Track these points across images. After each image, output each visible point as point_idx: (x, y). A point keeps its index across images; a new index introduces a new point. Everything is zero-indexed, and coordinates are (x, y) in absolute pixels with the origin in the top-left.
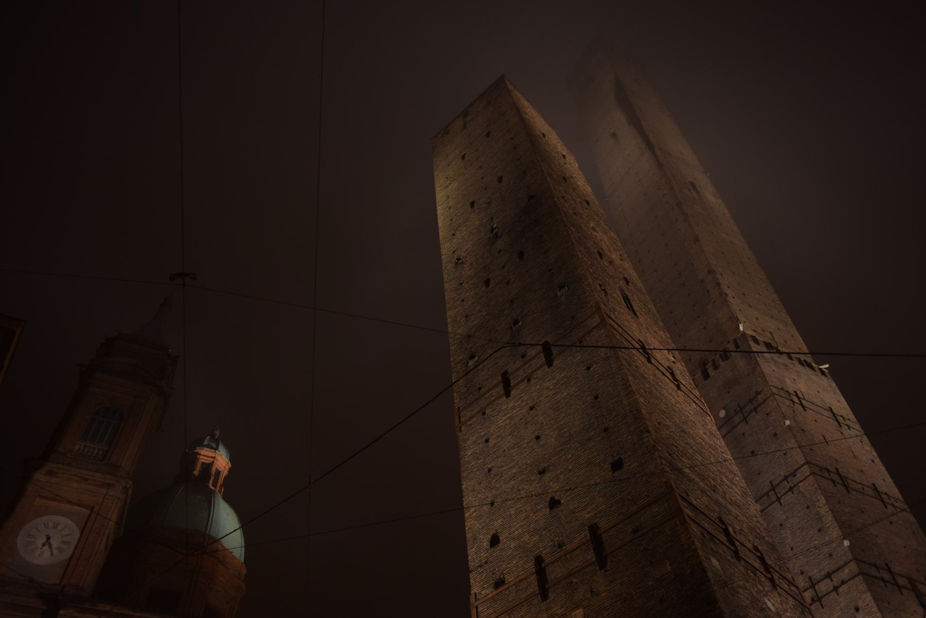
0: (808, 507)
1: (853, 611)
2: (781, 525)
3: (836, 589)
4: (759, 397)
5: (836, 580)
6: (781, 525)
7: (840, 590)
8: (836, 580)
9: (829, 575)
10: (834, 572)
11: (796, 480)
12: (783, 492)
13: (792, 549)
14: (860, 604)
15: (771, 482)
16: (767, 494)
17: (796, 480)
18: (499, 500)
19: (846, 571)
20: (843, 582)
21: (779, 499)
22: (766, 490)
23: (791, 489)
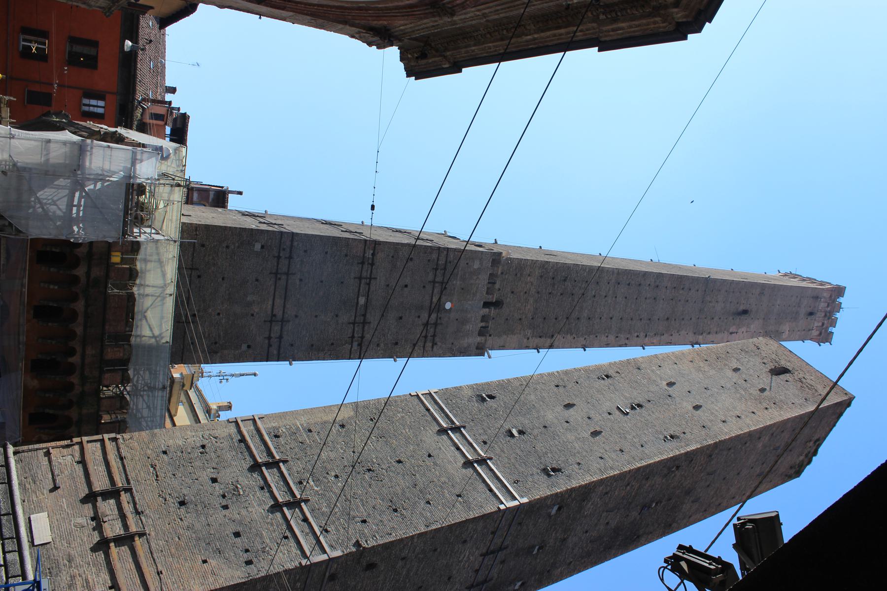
0: (332, 344)
1: (250, 343)
2: (337, 316)
3: (269, 338)
4: (431, 344)
5: (274, 341)
6: (337, 316)
7: (267, 341)
8: (274, 341)
9: (280, 337)
10: (280, 342)
11: (355, 344)
12: (356, 329)
13: (316, 316)
14: (251, 351)
15: (370, 323)
16: (364, 315)
17: (355, 344)
18: (400, 563)
19: (275, 352)
20: (270, 345)
21: (354, 323)
22: (368, 316)
23: (353, 337)
